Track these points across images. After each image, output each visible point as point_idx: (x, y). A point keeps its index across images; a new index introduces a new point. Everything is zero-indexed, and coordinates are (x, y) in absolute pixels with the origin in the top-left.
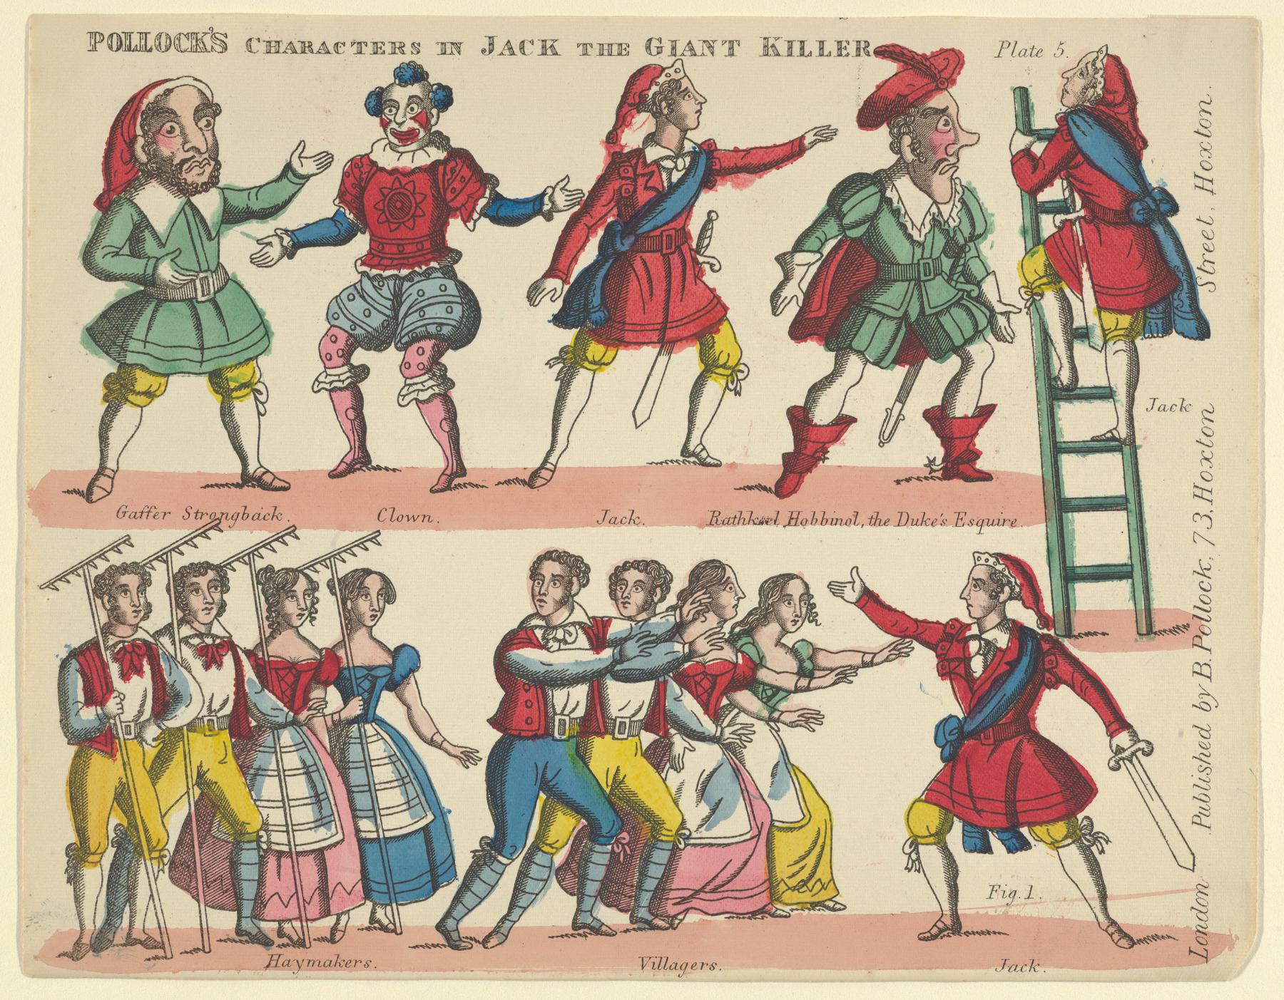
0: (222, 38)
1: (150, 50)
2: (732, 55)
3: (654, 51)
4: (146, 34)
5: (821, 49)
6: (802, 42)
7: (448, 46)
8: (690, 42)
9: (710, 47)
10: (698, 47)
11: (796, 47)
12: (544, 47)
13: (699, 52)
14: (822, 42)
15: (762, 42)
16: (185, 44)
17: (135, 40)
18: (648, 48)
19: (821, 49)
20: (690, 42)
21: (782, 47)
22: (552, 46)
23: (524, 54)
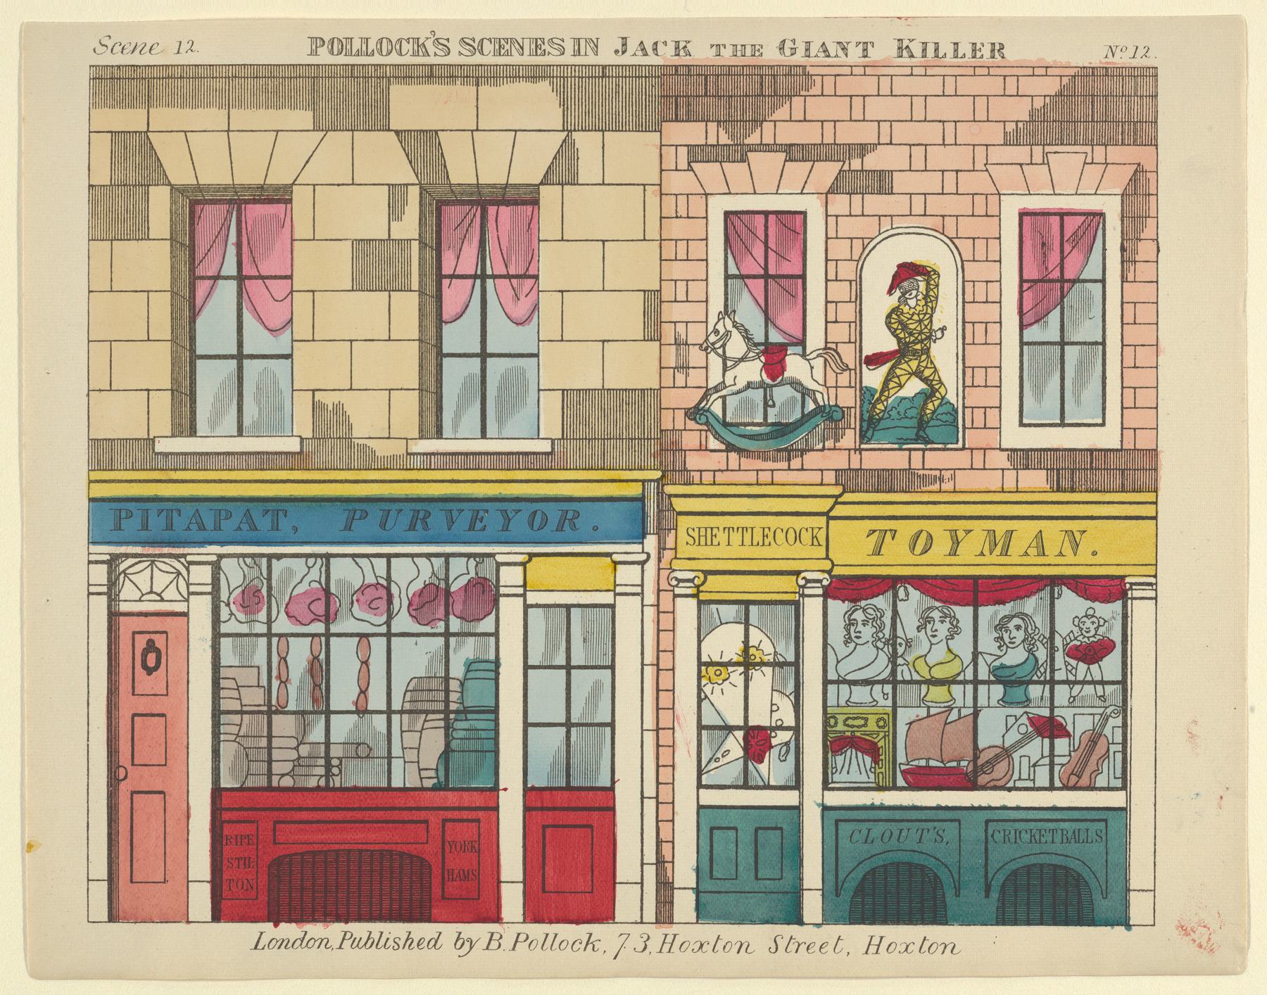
3: (788, 52)
4: (367, 39)
12: (677, 48)
17: (356, 45)
22: (685, 47)
23: (657, 55)
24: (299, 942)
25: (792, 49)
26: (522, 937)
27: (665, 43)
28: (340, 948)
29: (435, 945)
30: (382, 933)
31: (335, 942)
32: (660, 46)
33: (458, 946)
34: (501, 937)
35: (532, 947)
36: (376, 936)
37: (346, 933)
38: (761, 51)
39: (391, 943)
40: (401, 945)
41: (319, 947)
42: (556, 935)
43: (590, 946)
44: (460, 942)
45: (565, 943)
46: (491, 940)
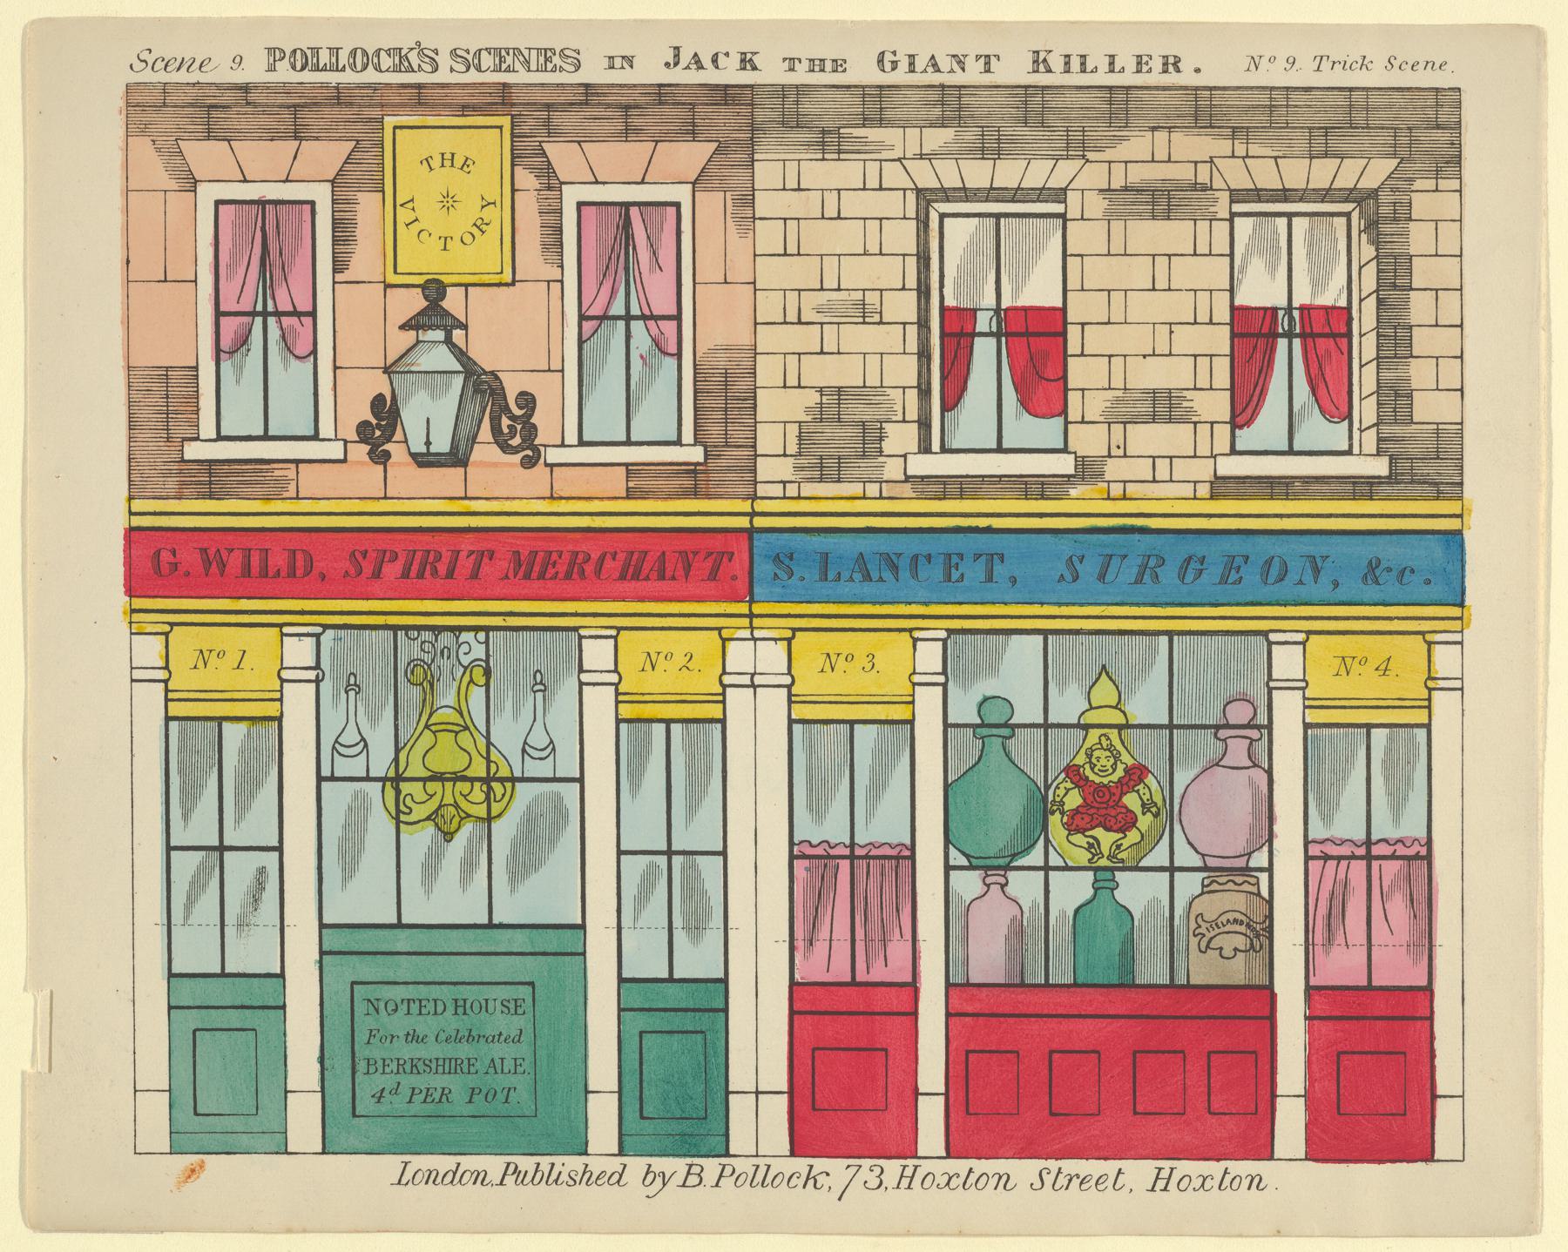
1: (343, 69)
2: (988, 71)
3: (888, 66)
5: (1112, 64)
6: (1083, 57)
8: (933, 57)
9: (960, 62)
10: (944, 63)
14: (1112, 57)
15: (1030, 57)
16: (386, 62)
18: (881, 61)
19: (1112, 64)
20: (933, 57)
25: (893, 62)
26: (728, 1170)
28: (501, 1184)
29: (618, 1182)
30: (553, 1165)
31: (495, 1175)
35: (739, 1183)
36: (545, 1168)
37: (508, 1164)
38: (844, 66)
39: (564, 1177)
40: (578, 1182)
41: (475, 1183)
42: (769, 1166)
43: (811, 1182)
44: (651, 1176)
46: (688, 1173)
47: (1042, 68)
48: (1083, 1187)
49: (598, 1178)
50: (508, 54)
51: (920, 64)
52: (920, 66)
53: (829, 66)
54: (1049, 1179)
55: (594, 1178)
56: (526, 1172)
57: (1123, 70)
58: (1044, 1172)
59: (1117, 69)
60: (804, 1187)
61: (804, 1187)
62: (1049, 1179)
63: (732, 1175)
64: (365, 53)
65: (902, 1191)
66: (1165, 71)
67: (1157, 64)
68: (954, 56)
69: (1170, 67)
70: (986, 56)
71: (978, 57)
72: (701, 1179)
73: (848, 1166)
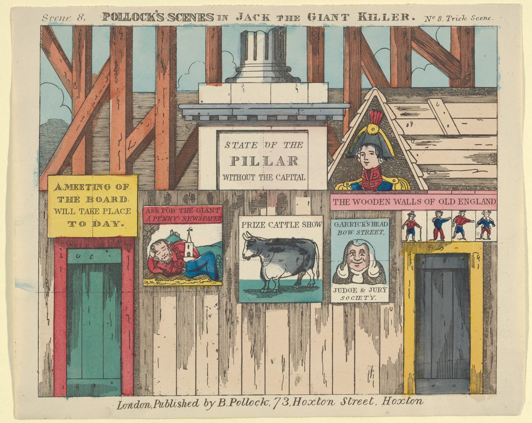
0: (162, 15)
2: (345, 20)
3: (312, 18)
5: (384, 17)
7: (222, 17)
8: (327, 15)
10: (330, 17)
11: (373, 16)
13: (331, 19)
17: (123, 16)
18: (309, 17)
20: (327, 15)
21: (367, 16)
24: (137, 405)
25: (314, 17)
26: (234, 400)
27: (259, 15)
29: (196, 405)
30: (172, 400)
32: (257, 17)
33: (206, 405)
34: (225, 400)
35: (238, 404)
36: (170, 402)
37: (156, 401)
38: (299, 18)
39: (177, 404)
40: (181, 406)
43: (263, 404)
44: (207, 403)
45: (253, 402)
47: (362, 19)
48: (359, 403)
49: (188, 404)
50: (189, 16)
51: (323, 17)
52: (323, 18)
53: (293, 18)
54: (347, 401)
55: (187, 404)
56: (163, 403)
57: (379, 20)
58: (345, 399)
59: (386, 19)
60: (261, 405)
61: (261, 405)
62: (347, 401)
63: (235, 402)
64: (138, 15)
65: (296, 406)
66: (403, 20)
67: (400, 17)
68: (333, 15)
69: (405, 18)
70: (345, 15)
71: (342, 15)
72: (225, 403)
73: (276, 398)
